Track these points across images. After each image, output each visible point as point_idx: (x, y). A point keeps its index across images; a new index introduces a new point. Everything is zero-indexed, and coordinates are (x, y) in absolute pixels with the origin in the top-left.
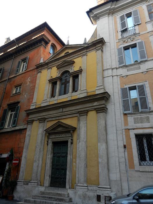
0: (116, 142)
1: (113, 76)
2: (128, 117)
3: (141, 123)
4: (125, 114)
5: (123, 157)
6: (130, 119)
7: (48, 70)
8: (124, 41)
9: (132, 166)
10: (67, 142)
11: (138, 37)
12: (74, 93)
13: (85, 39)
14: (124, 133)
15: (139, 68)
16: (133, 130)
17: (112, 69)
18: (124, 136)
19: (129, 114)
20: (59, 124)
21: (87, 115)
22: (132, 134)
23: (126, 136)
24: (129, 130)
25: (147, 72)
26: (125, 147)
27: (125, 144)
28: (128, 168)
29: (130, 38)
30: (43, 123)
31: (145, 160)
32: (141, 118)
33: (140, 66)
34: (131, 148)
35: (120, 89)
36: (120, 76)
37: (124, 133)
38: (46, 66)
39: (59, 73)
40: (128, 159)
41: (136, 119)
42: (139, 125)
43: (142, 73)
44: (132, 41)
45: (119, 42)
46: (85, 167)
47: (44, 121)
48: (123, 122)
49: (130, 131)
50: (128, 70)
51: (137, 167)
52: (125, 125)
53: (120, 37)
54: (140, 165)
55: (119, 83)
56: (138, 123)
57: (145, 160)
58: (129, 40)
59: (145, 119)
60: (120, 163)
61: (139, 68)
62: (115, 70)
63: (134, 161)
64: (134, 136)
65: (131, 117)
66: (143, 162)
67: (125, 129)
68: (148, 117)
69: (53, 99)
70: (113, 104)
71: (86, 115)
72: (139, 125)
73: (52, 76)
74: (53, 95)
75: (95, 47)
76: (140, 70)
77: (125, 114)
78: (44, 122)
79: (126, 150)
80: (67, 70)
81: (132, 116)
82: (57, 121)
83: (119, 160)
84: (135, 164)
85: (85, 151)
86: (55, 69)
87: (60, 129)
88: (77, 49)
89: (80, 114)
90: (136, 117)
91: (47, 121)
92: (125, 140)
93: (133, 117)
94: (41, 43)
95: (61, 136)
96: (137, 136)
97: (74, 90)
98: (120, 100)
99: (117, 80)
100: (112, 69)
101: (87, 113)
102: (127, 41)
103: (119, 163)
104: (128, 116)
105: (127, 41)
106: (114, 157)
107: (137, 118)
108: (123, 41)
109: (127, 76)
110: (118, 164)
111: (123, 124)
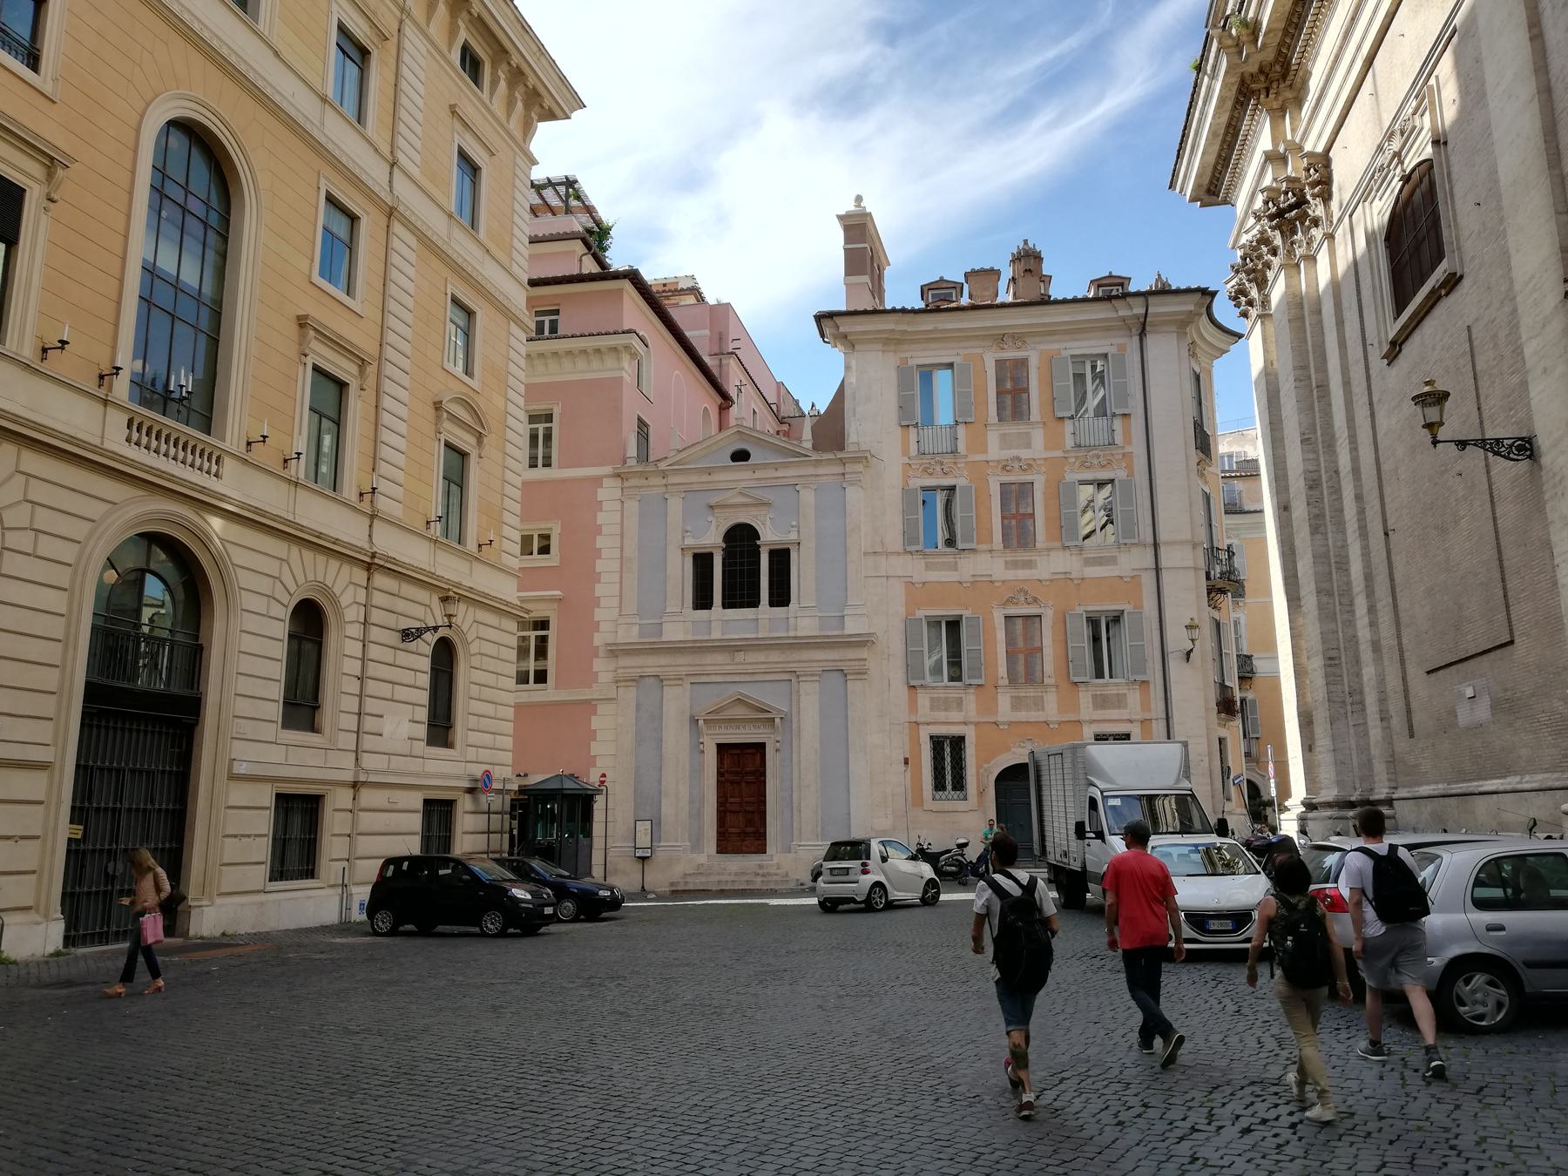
6: (923, 699)
9: (918, 801)
10: (762, 746)
15: (955, 568)
17: (888, 554)
26: (906, 762)
31: (944, 788)
50: (928, 567)
51: (929, 803)
53: (913, 450)
57: (944, 788)
61: (955, 568)
69: (703, 613)
72: (941, 715)
87: (740, 712)
92: (907, 747)
94: (619, 360)
97: (781, 596)
99: (898, 591)
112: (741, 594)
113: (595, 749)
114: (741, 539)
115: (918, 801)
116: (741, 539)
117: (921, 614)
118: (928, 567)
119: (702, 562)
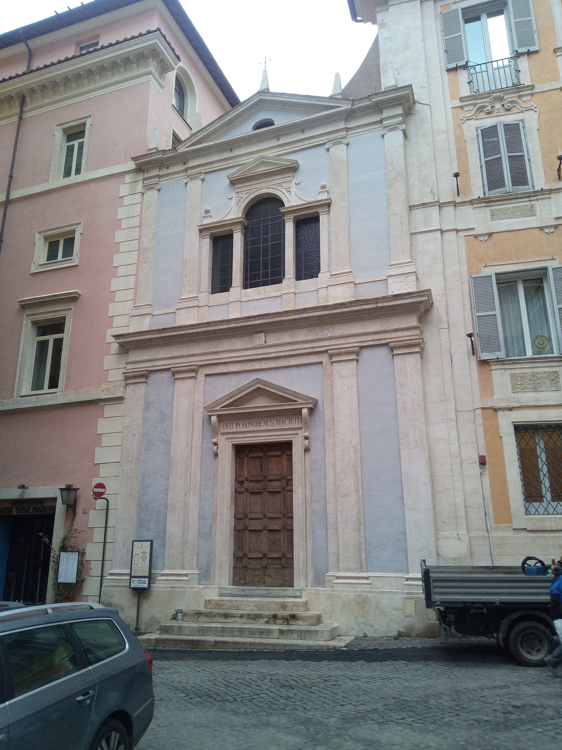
0: (454, 448)
1: (442, 232)
2: (492, 371)
3: (535, 390)
4: (484, 363)
5: (479, 493)
7: (191, 184)
8: (481, 109)
9: (502, 514)
10: (287, 446)
11: (529, 98)
12: (307, 284)
13: (338, 77)
14: (480, 421)
15: (531, 212)
16: (507, 413)
17: (441, 206)
18: (480, 429)
19: (498, 361)
20: (259, 386)
21: (357, 361)
22: (506, 423)
23: (486, 430)
24: (496, 410)
25: (556, 227)
26: (482, 462)
27: (483, 453)
28: (492, 521)
29: (501, 99)
30: (192, 381)
31: (540, 498)
32: (534, 374)
33: (532, 207)
34: (503, 467)
35: (466, 278)
36: (466, 233)
37: (481, 421)
38: (177, 163)
39: (239, 201)
40: (493, 498)
41: (519, 379)
42: (529, 397)
43: (541, 229)
44: (508, 110)
45: (461, 107)
46: (360, 523)
47: (193, 374)
48: (476, 386)
49: (500, 413)
50: (493, 216)
52: (483, 396)
54: (527, 512)
55: (464, 257)
56: (524, 390)
57: (540, 498)
58: (498, 106)
59: (547, 381)
60: (469, 509)
61: (531, 212)
62: (449, 211)
63: (511, 502)
64: (512, 430)
65: (503, 371)
66: (536, 504)
67: (483, 409)
68: (556, 372)
69: (221, 297)
70: (445, 326)
71: (355, 359)
72: (529, 397)
73: (207, 208)
74: (221, 282)
75: (377, 118)
76: (534, 218)
77: (484, 363)
78: (195, 378)
79: (487, 472)
80: (271, 191)
81: (505, 369)
82: (252, 377)
83: (465, 500)
84: (512, 511)
85: (356, 473)
86: (221, 181)
88: (310, 113)
89: (331, 356)
90: (517, 371)
91: (207, 375)
92: (482, 442)
93: (509, 372)
95: (264, 427)
96: (520, 429)
97: (308, 267)
98: (468, 312)
99: (455, 245)
100: (441, 206)
101: (358, 354)
102: (489, 108)
103: (466, 507)
104: (493, 367)
105: (489, 108)
106: (452, 490)
107: (523, 376)
108: (475, 105)
109: (490, 235)
110: (463, 513)
111: (477, 392)
112: (263, 270)
113: (100, 456)
114: (263, 212)
115: (502, 514)
116: (263, 212)
117: (491, 271)
118: (493, 216)
119: (221, 241)
